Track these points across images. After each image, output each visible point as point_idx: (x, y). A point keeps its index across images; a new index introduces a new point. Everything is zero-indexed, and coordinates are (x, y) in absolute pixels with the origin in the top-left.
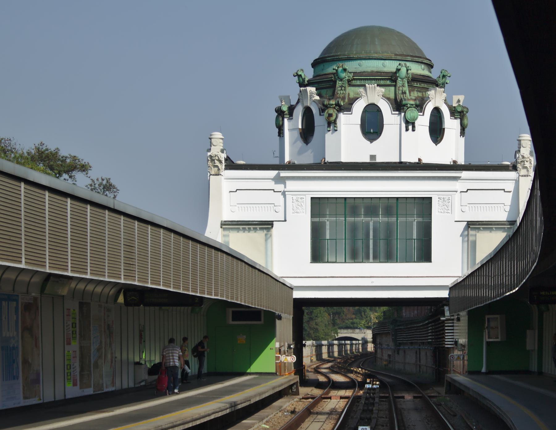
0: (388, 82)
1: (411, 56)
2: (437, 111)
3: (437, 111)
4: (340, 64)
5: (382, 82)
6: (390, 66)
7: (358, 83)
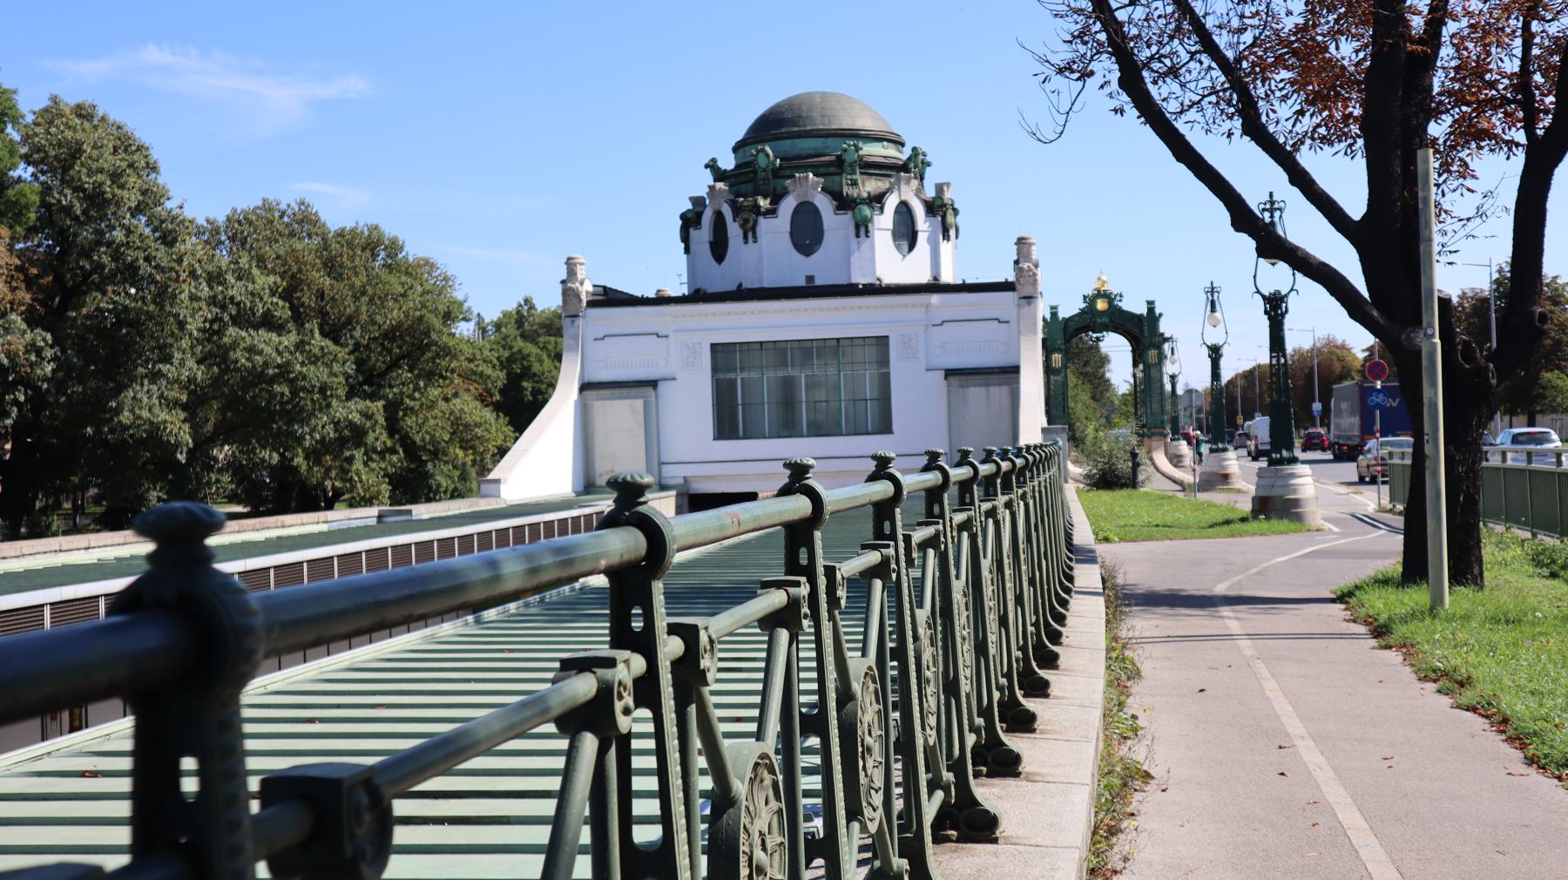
0: (832, 170)
5: (822, 170)
6: (836, 147)
7: (788, 172)
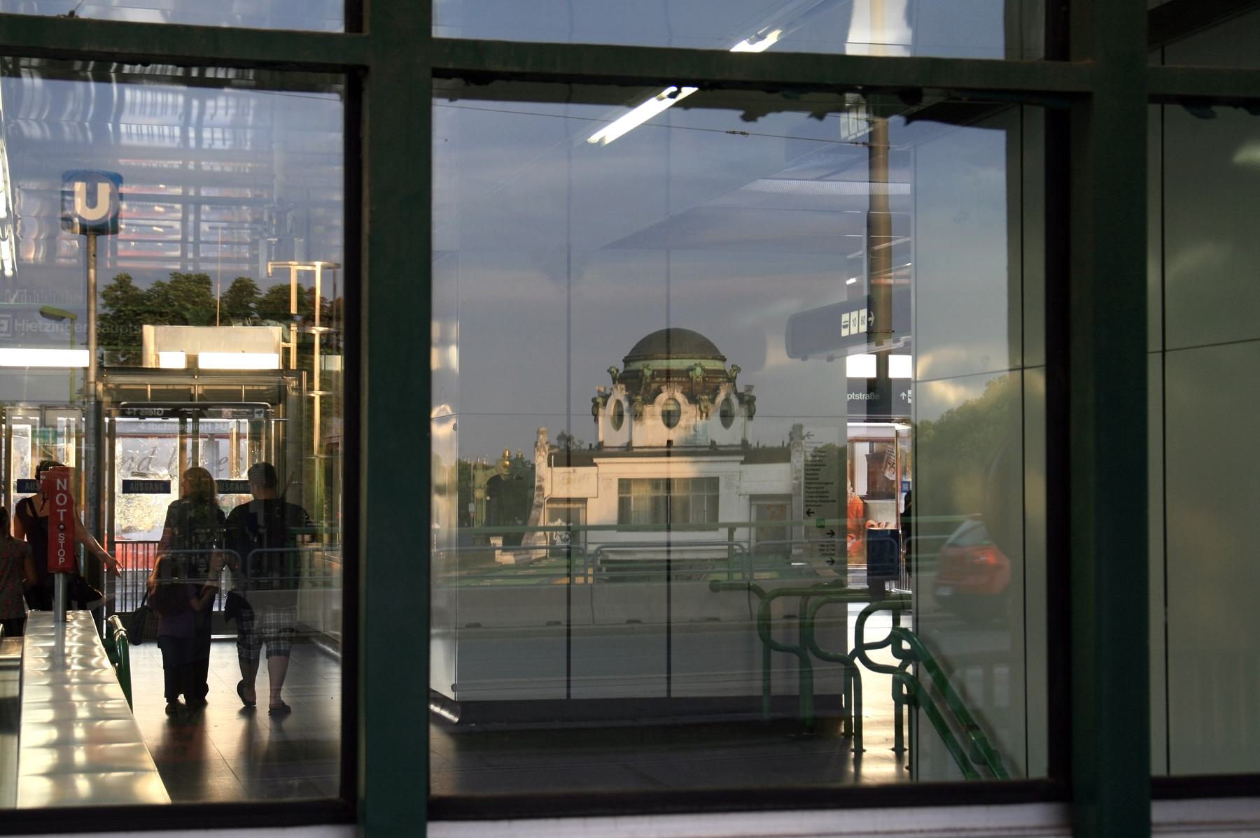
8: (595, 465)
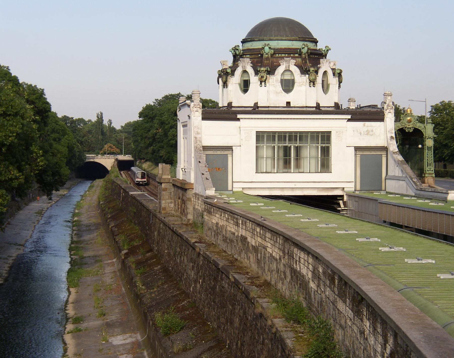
0: (297, 55)
1: (308, 38)
2: (325, 73)
3: (325, 73)
4: (267, 42)
8: (238, 120)
